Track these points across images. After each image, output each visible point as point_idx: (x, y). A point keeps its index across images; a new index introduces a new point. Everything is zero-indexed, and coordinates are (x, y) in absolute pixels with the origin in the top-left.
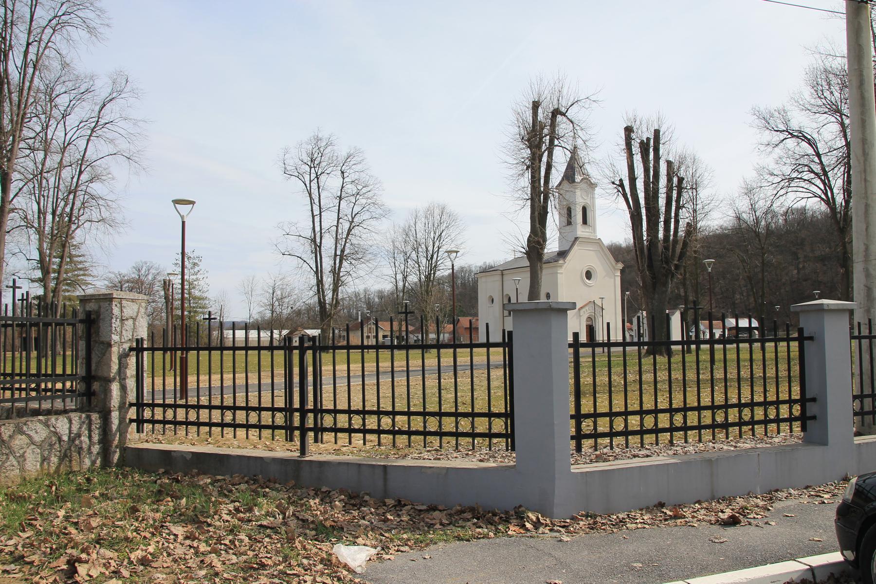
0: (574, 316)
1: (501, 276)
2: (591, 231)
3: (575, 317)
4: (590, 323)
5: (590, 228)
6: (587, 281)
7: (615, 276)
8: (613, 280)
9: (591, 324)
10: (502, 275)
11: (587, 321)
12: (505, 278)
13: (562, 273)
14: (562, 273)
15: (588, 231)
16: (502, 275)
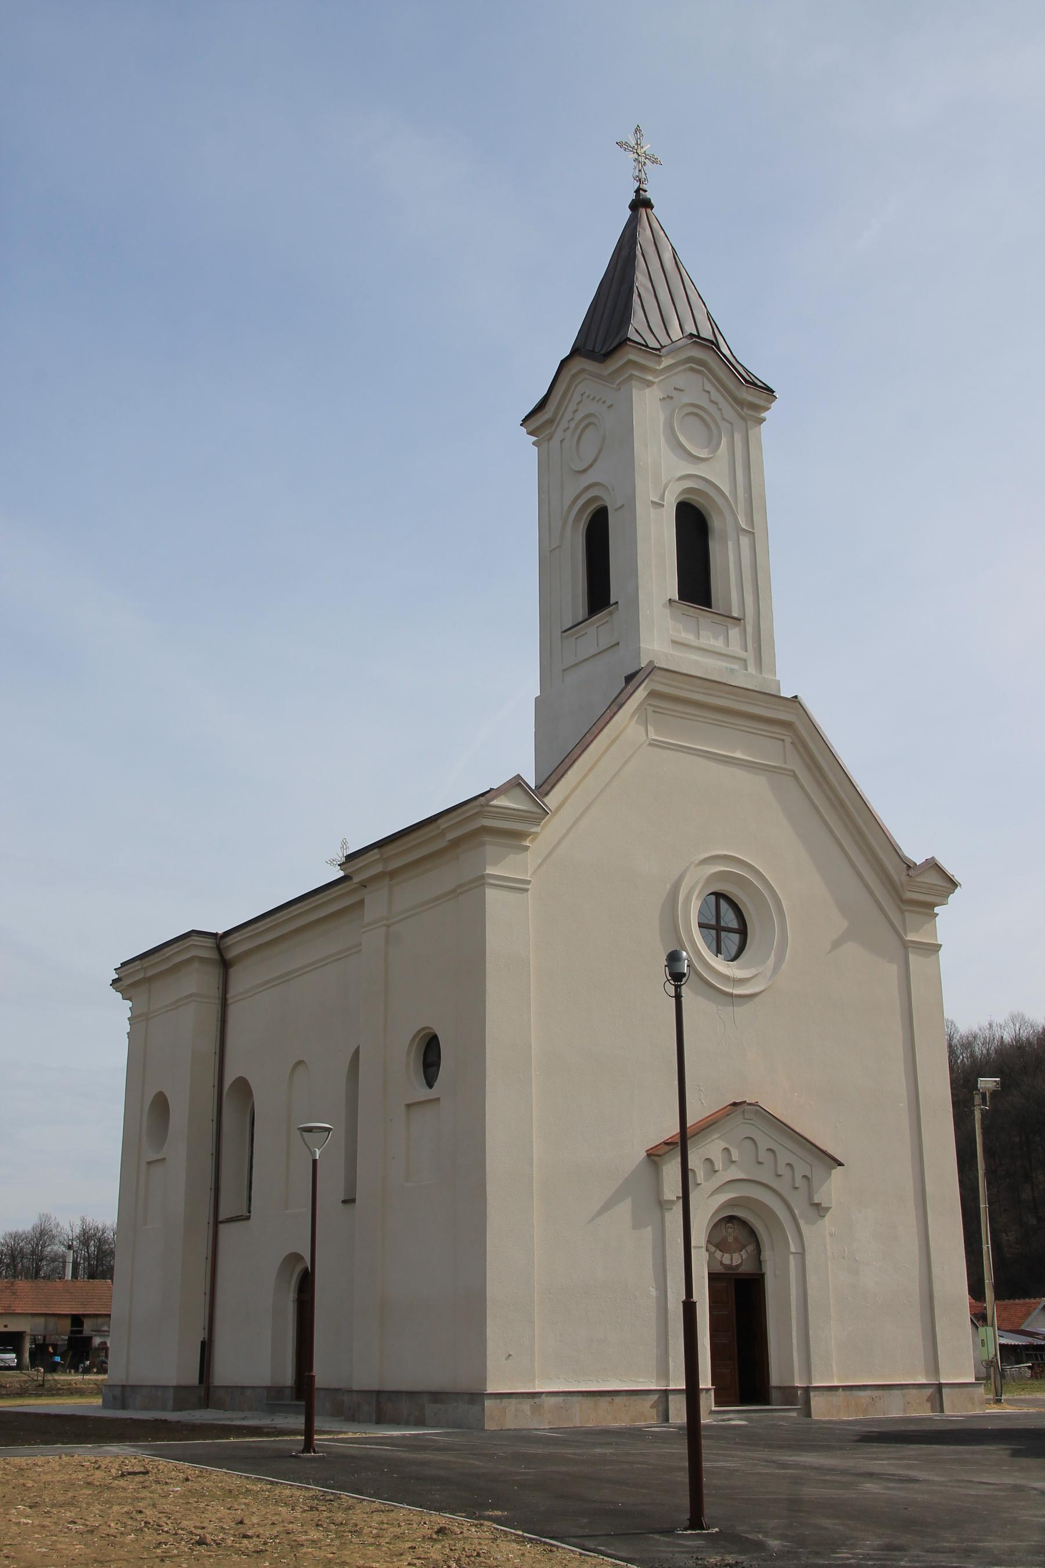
0: (605, 1208)
1: (211, 978)
2: (735, 649)
3: (625, 1207)
4: (736, 1260)
5: (734, 633)
6: (719, 964)
7: (906, 946)
8: (892, 970)
9: (747, 1268)
10: (225, 965)
11: (717, 1242)
12: (242, 980)
13: (519, 887)
14: (519, 887)
15: (718, 644)
16: (225, 965)
